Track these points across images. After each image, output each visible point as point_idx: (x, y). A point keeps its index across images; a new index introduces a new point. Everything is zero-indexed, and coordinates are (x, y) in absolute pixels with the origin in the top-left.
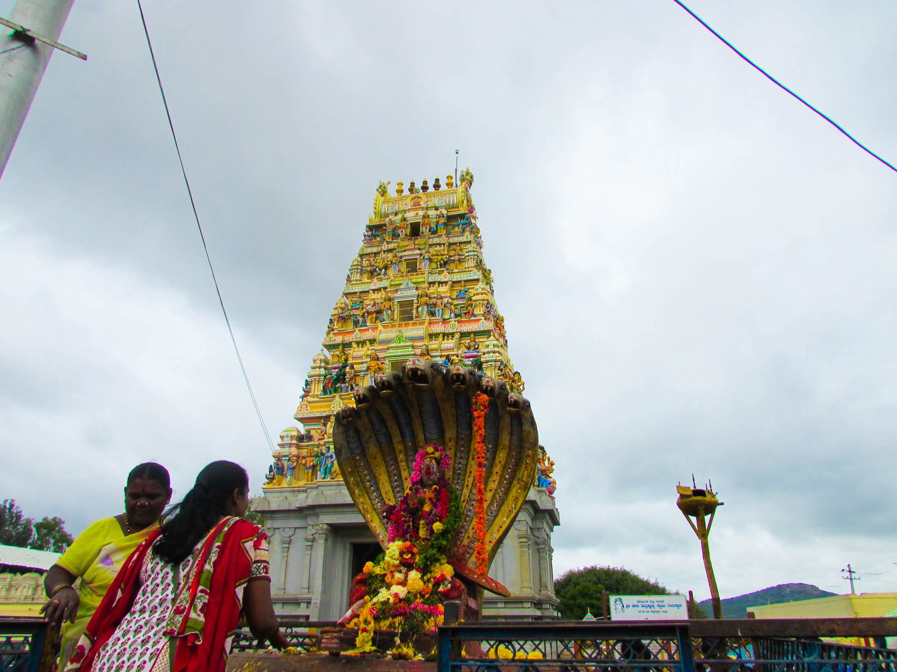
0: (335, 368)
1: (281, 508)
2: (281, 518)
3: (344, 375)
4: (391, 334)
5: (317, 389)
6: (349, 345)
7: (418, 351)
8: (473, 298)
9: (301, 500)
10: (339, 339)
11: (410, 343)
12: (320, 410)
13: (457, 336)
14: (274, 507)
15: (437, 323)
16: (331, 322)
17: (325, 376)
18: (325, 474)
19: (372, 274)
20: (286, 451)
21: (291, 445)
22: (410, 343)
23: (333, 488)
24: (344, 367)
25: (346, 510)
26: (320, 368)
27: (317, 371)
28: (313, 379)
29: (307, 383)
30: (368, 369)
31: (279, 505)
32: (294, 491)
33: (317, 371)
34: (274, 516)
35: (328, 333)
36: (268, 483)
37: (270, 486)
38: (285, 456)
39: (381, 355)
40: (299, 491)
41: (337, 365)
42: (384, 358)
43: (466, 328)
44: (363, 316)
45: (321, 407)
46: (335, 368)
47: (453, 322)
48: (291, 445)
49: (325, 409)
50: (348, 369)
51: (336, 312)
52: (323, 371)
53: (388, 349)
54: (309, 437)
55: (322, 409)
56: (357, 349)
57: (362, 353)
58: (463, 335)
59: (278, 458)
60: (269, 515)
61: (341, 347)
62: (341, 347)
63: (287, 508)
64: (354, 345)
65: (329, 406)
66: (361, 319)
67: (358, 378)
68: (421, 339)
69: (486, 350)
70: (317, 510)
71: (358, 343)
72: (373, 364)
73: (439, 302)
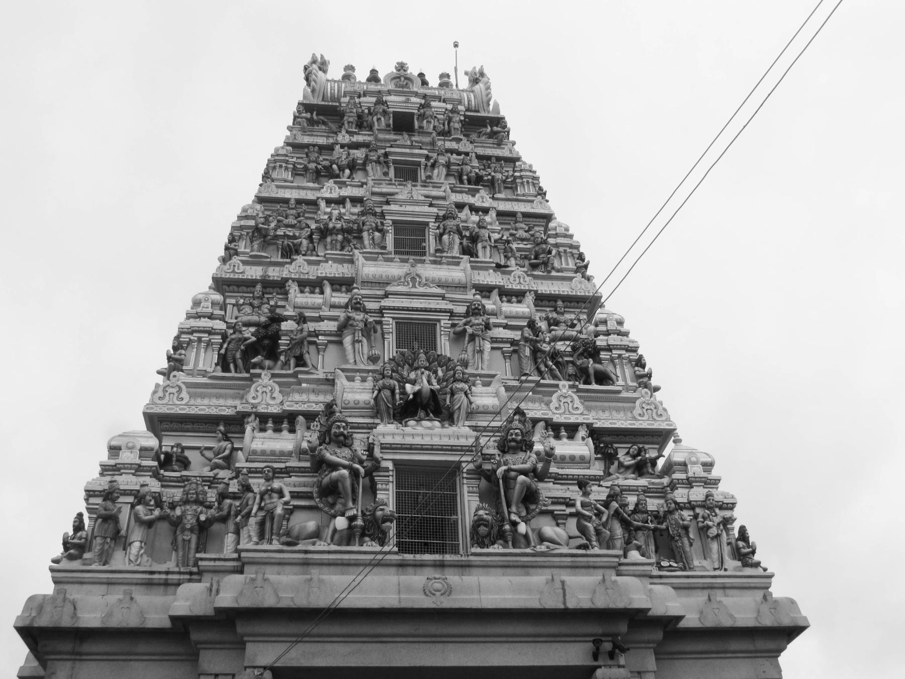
0: (248, 324)
1: (115, 622)
2: (107, 657)
3: (276, 336)
4: (395, 269)
5: (204, 360)
6: (280, 286)
7: (462, 309)
8: (551, 241)
9: (189, 599)
10: (254, 272)
11: (439, 291)
12: (214, 401)
13: (530, 299)
14: (90, 619)
15: (486, 269)
16: (232, 239)
17: (224, 336)
18: (261, 536)
19: (322, 174)
20: (127, 481)
21: (139, 469)
22: (439, 291)
23: (287, 569)
24: (277, 319)
25: (336, 629)
26: (211, 317)
27: (205, 323)
28: (194, 337)
29: (178, 346)
30: (345, 326)
31: (110, 615)
32: (149, 584)
33: (205, 323)
34: (87, 647)
35: (224, 260)
36: (71, 558)
37: (76, 565)
38: (125, 493)
39: (371, 305)
40: (166, 584)
41: (255, 318)
42: (381, 311)
43: (546, 287)
44: (310, 238)
45: (218, 397)
46: (248, 324)
47: (519, 272)
48: (139, 469)
49: (230, 402)
50: (286, 326)
51: (252, 223)
52: (219, 325)
53: (386, 295)
54: (185, 464)
55: (221, 402)
56: (299, 295)
57: (321, 301)
58: (542, 300)
59: (104, 498)
60: (67, 646)
61: (259, 287)
62: (259, 287)
63: (133, 622)
64: (293, 289)
65: (242, 398)
66: (305, 242)
67: (312, 348)
68: (461, 287)
69: (602, 328)
70: (241, 629)
71: (303, 284)
72: (359, 316)
73: (484, 233)
